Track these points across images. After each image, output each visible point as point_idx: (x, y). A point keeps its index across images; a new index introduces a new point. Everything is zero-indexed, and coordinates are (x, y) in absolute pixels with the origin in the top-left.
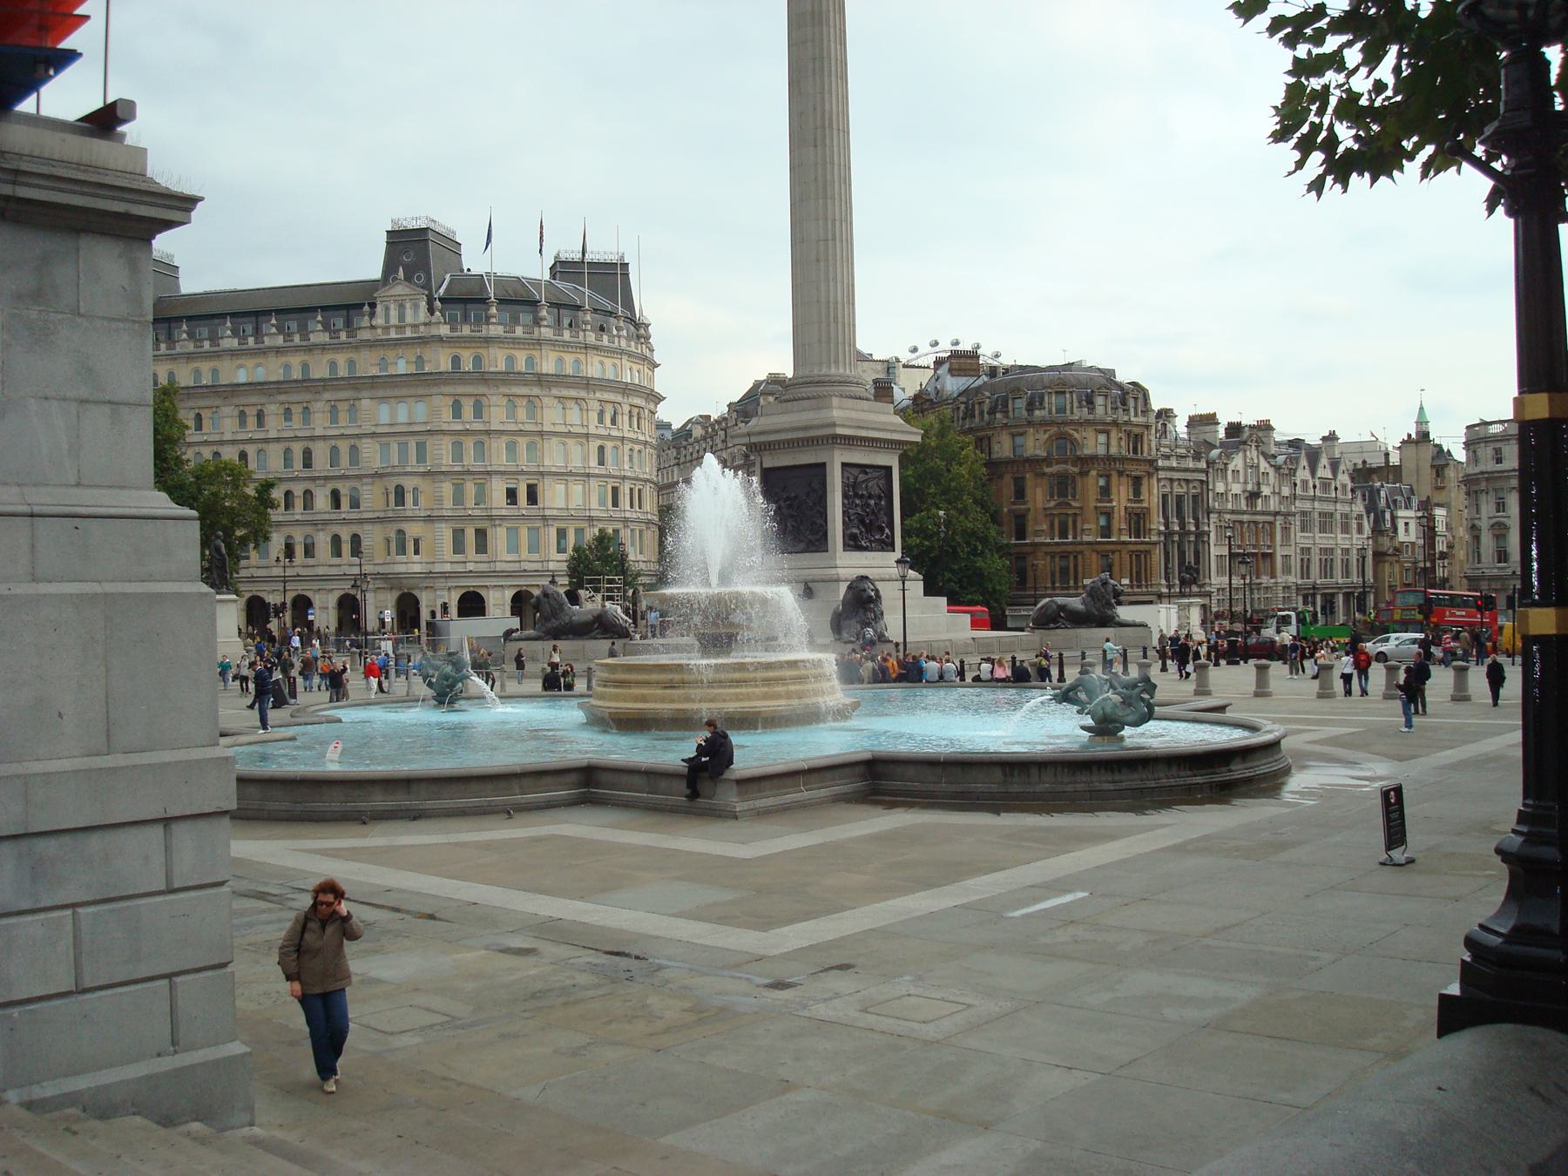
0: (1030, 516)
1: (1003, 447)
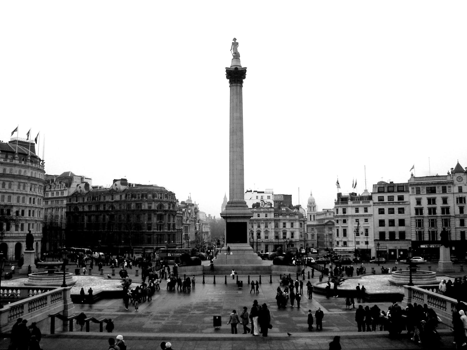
0: (153, 224)
1: (145, 206)
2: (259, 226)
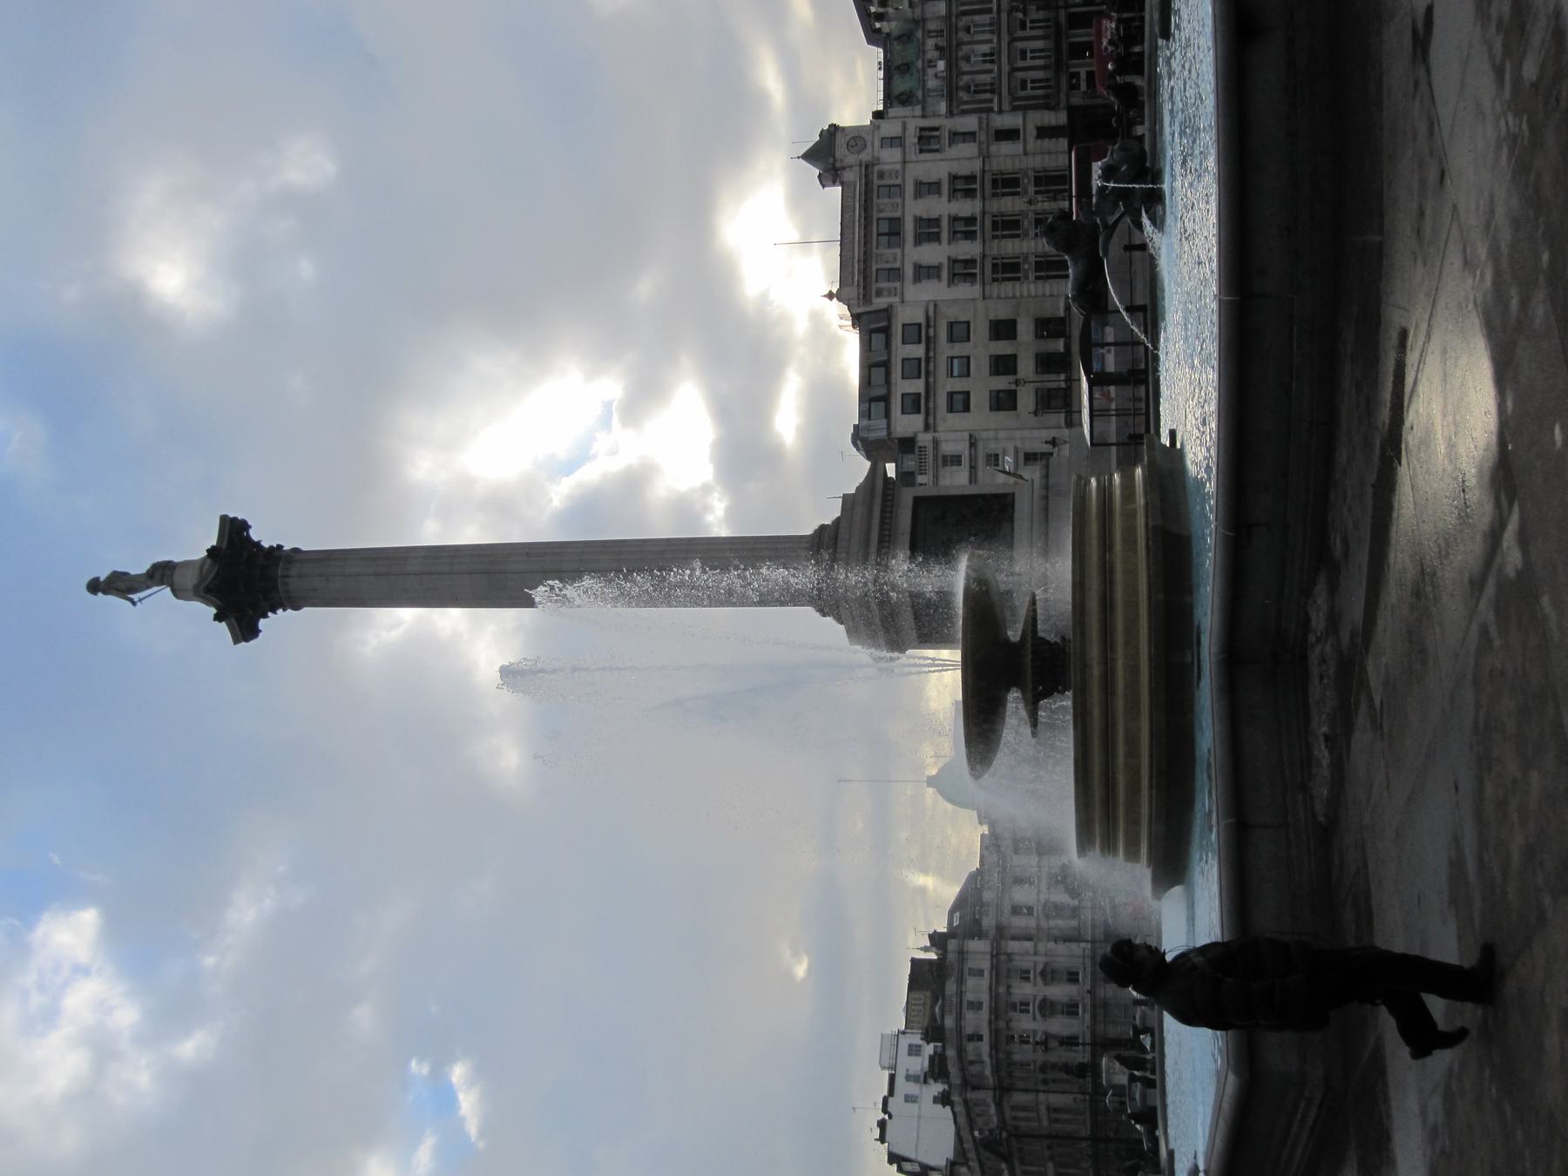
2: (1024, 1007)
